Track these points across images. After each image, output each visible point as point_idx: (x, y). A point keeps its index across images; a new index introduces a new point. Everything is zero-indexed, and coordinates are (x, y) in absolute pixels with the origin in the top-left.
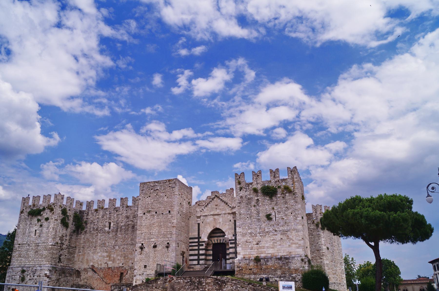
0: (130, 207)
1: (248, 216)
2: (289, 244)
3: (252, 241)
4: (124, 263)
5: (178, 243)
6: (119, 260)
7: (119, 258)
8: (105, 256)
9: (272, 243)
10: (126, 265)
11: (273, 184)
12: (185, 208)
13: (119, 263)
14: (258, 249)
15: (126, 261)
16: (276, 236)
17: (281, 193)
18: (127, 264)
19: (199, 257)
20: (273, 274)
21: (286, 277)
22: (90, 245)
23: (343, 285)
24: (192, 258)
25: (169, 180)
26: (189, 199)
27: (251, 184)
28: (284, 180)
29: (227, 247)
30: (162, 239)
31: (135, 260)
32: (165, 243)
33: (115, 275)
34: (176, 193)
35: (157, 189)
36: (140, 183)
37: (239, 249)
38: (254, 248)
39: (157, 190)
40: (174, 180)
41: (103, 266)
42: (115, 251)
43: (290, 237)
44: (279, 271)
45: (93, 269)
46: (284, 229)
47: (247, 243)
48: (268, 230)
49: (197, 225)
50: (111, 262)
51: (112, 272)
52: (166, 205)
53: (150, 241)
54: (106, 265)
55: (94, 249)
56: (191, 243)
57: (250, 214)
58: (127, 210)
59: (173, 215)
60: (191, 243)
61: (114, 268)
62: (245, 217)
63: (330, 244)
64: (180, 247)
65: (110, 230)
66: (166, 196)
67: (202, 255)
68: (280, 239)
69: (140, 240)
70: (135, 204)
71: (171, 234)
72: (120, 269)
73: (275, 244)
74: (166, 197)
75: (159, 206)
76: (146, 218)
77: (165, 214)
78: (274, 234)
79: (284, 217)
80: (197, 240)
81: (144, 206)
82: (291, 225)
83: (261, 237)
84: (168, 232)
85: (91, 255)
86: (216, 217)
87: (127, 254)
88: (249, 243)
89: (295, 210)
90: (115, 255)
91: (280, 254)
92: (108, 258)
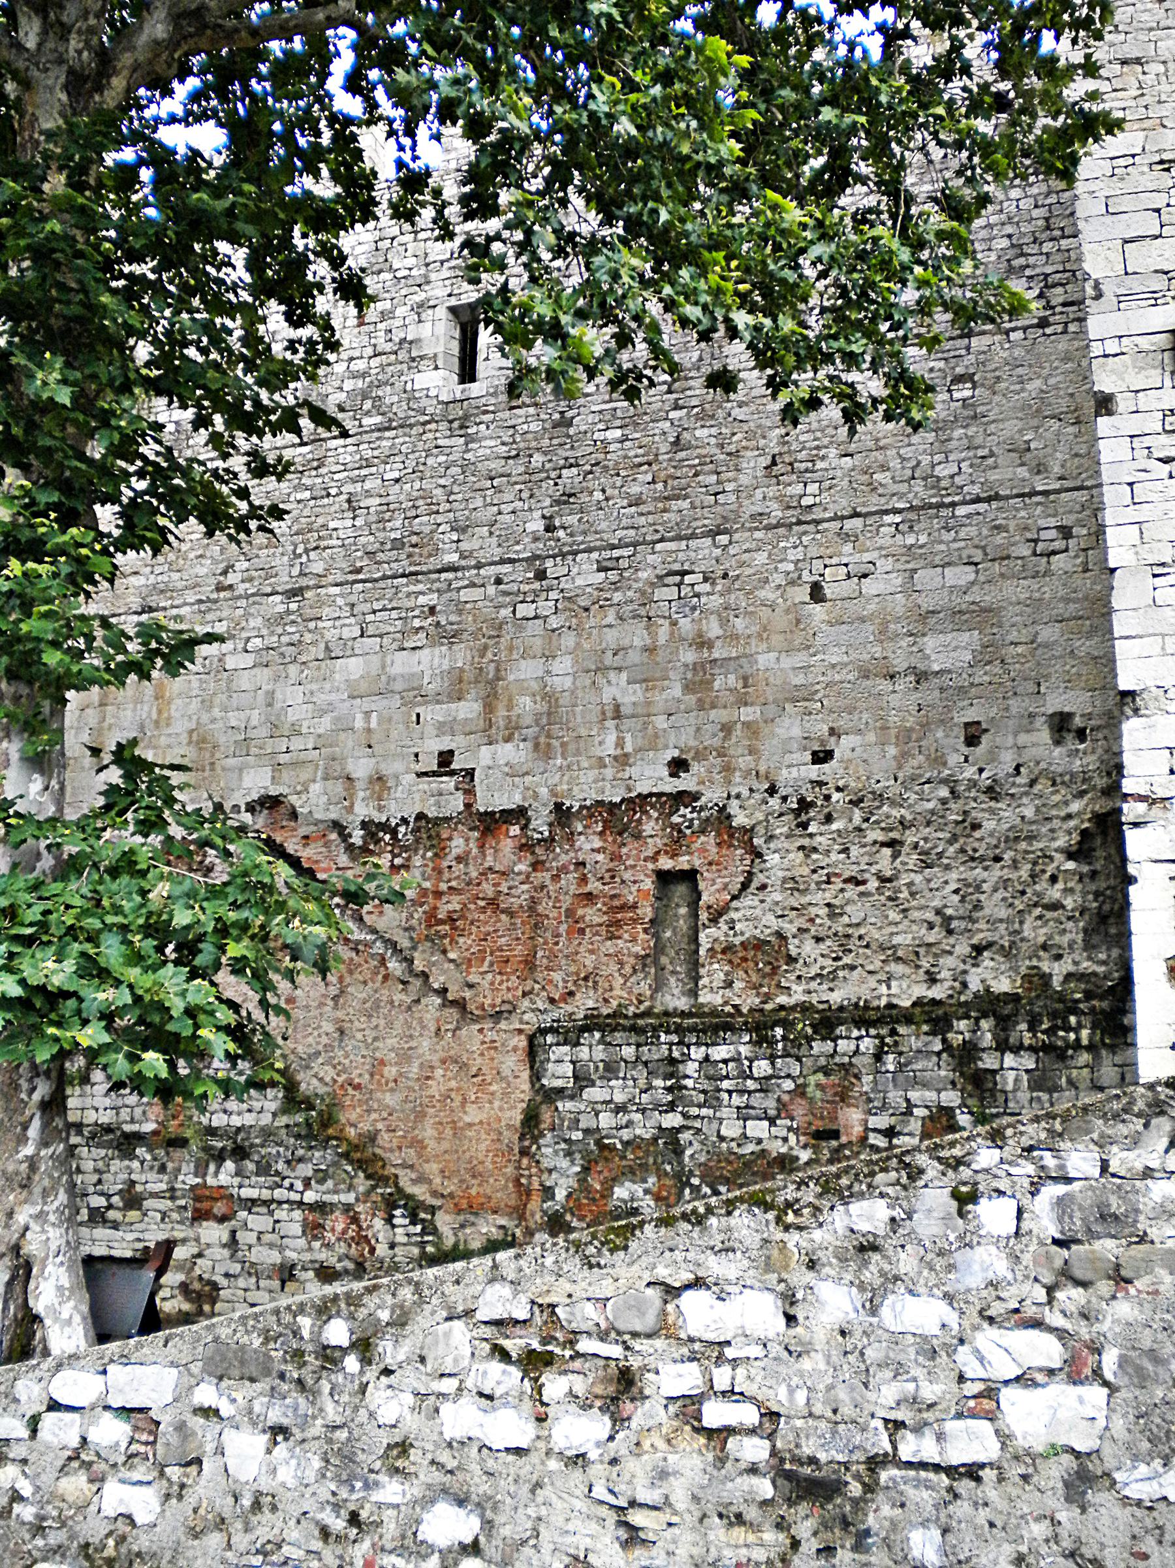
10: (728, 769)
13: (623, 760)
15: (727, 729)
18: (745, 762)
22: (232, 578)
42: (554, 622)
50: (510, 753)
51: (536, 865)
54: (449, 783)
65: (475, 389)
85: (244, 681)
90: (562, 665)
92: (468, 709)
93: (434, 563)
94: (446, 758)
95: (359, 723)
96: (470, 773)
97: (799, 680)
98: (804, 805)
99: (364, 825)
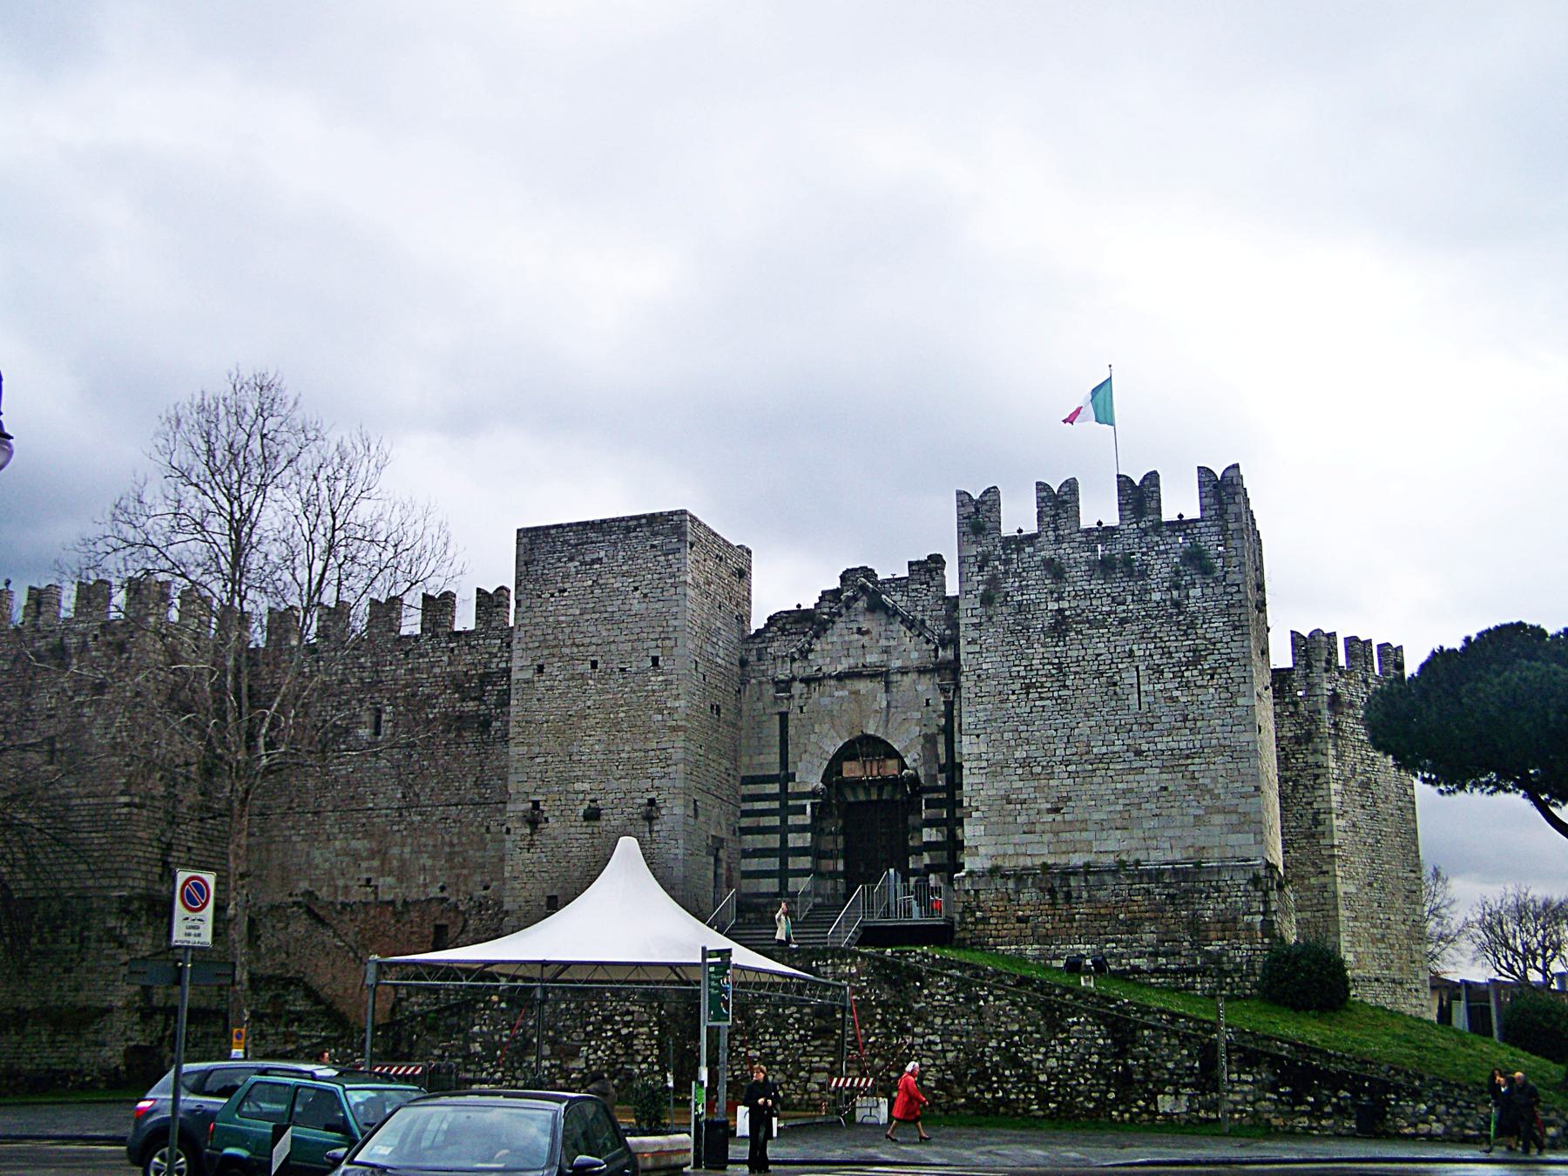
0: (467, 634)
1: (1013, 687)
2: (1202, 812)
3: (1032, 796)
4: (449, 885)
5: (695, 801)
6: (424, 868)
7: (426, 860)
8: (365, 854)
9: (1119, 808)
10: (458, 891)
11: (1131, 541)
12: (720, 643)
13: (425, 885)
14: (1056, 833)
16: (1138, 778)
17: (1166, 584)
18: (463, 888)
19: (784, 863)
20: (1121, 940)
21: (1179, 953)
23: (1417, 990)
24: (754, 864)
25: (652, 518)
26: (737, 605)
27: (1031, 539)
28: (1181, 524)
29: (912, 820)
30: (624, 784)
31: (507, 875)
32: (639, 801)
33: (412, 933)
34: (682, 579)
35: (595, 556)
36: (519, 531)
37: (970, 832)
38: (1038, 827)
39: (593, 562)
40: (675, 518)
41: (357, 895)
43: (1201, 781)
44: (1147, 926)
45: (311, 909)
46: (1174, 745)
47: (1012, 806)
48: (1104, 750)
49: (777, 717)
50: (390, 880)
51: (398, 921)
52: (639, 630)
53: (568, 792)
54: (369, 890)
55: (309, 824)
56: (746, 798)
57: (1024, 678)
58: (452, 650)
59: (670, 677)
60: (746, 798)
61: (405, 903)
62: (1000, 688)
63: (1363, 807)
64: (701, 818)
66: (636, 589)
67: (801, 852)
68: (1156, 789)
69: (526, 788)
70: (488, 622)
71: (666, 761)
72: (434, 907)
73: (1135, 813)
74: (637, 594)
75: (604, 633)
76: (551, 688)
77: (634, 669)
78: (1131, 769)
79: (1176, 693)
80: (774, 788)
81: (539, 633)
82: (1209, 730)
83: (1070, 781)
84: (652, 753)
85: (298, 847)
86: (863, 686)
87: (461, 843)
88: (1018, 806)
89: (1229, 664)
90: (407, 849)
91: (1156, 857)
92: (376, 863)
93: (364, 806)
94: (369, 880)
95: (339, 866)
96: (376, 887)
97: (481, 861)
98: (481, 904)
99: (342, 903)
